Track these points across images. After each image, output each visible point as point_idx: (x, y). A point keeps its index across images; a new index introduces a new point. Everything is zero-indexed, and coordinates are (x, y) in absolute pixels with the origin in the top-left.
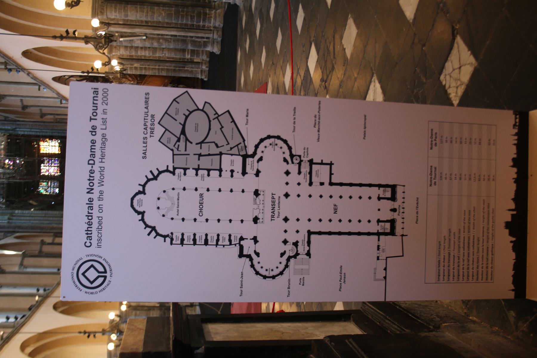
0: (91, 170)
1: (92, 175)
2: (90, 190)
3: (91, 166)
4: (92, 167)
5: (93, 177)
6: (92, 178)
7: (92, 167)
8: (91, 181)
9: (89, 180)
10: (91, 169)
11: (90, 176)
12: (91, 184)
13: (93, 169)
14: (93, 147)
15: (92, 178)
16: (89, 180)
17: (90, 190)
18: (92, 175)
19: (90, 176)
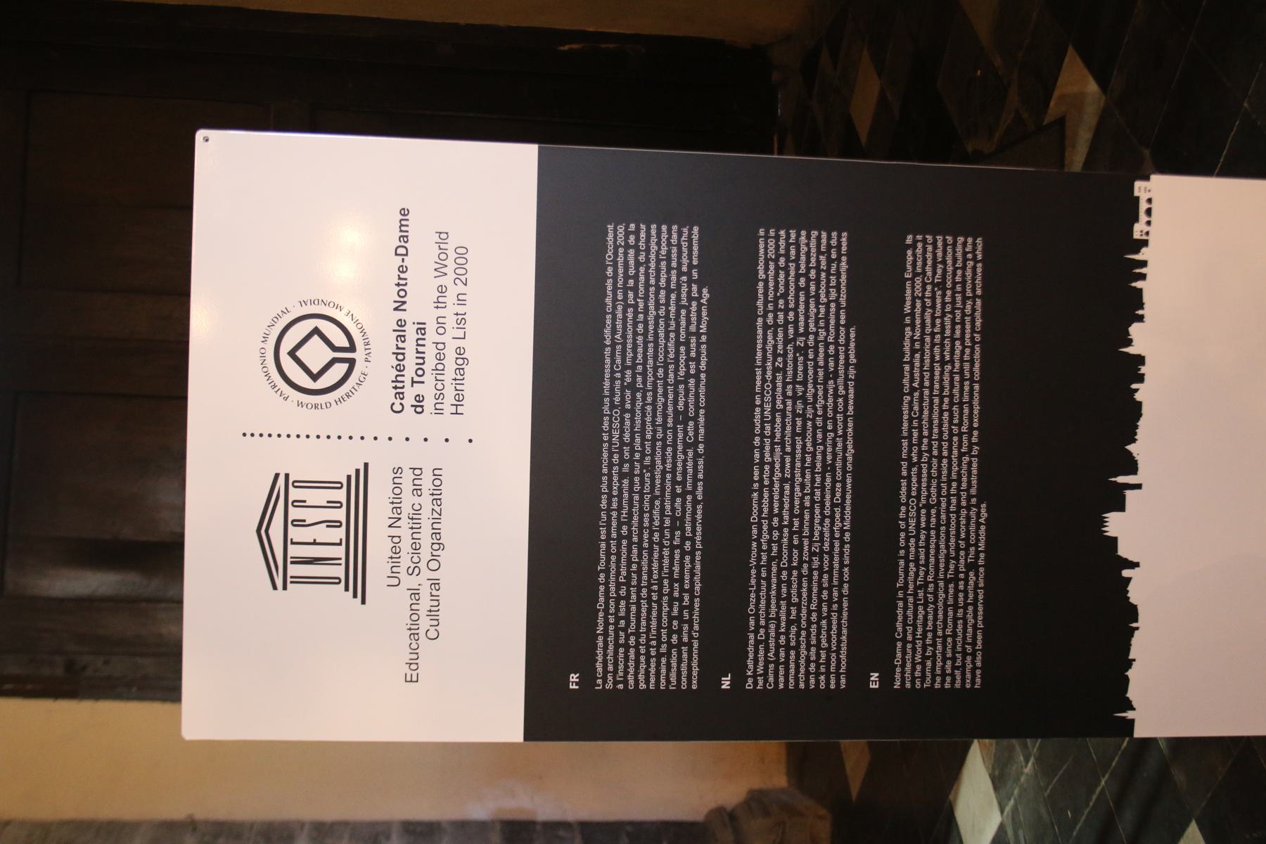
0: (402, 266)
1: (402, 276)
2: (400, 304)
3: (401, 257)
4: (403, 260)
5: (406, 279)
6: (402, 282)
7: (403, 260)
8: (401, 287)
9: (398, 285)
10: (402, 264)
11: (400, 278)
12: (402, 293)
13: (404, 264)
14: (403, 223)
15: (402, 282)
16: (398, 285)
17: (400, 304)
18: (402, 276)
19: (400, 278)
